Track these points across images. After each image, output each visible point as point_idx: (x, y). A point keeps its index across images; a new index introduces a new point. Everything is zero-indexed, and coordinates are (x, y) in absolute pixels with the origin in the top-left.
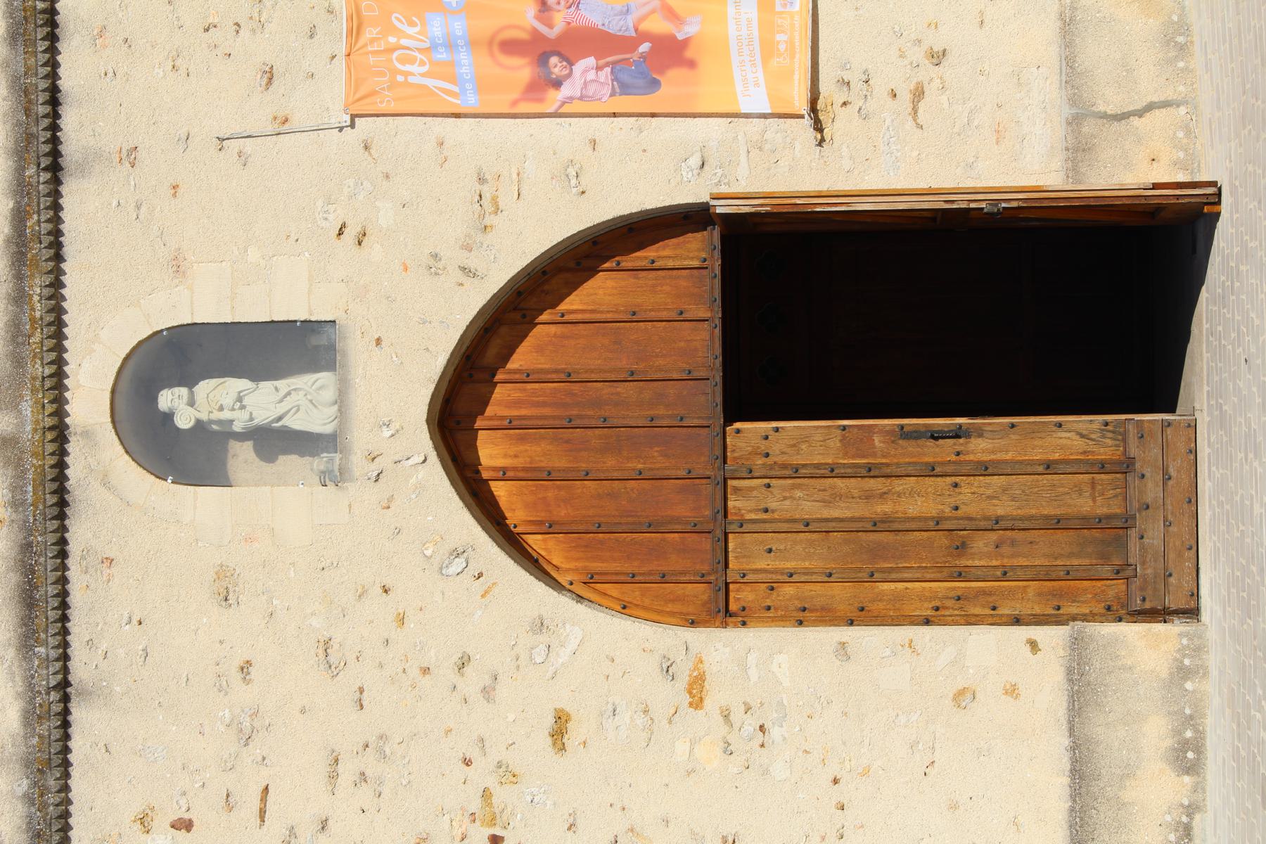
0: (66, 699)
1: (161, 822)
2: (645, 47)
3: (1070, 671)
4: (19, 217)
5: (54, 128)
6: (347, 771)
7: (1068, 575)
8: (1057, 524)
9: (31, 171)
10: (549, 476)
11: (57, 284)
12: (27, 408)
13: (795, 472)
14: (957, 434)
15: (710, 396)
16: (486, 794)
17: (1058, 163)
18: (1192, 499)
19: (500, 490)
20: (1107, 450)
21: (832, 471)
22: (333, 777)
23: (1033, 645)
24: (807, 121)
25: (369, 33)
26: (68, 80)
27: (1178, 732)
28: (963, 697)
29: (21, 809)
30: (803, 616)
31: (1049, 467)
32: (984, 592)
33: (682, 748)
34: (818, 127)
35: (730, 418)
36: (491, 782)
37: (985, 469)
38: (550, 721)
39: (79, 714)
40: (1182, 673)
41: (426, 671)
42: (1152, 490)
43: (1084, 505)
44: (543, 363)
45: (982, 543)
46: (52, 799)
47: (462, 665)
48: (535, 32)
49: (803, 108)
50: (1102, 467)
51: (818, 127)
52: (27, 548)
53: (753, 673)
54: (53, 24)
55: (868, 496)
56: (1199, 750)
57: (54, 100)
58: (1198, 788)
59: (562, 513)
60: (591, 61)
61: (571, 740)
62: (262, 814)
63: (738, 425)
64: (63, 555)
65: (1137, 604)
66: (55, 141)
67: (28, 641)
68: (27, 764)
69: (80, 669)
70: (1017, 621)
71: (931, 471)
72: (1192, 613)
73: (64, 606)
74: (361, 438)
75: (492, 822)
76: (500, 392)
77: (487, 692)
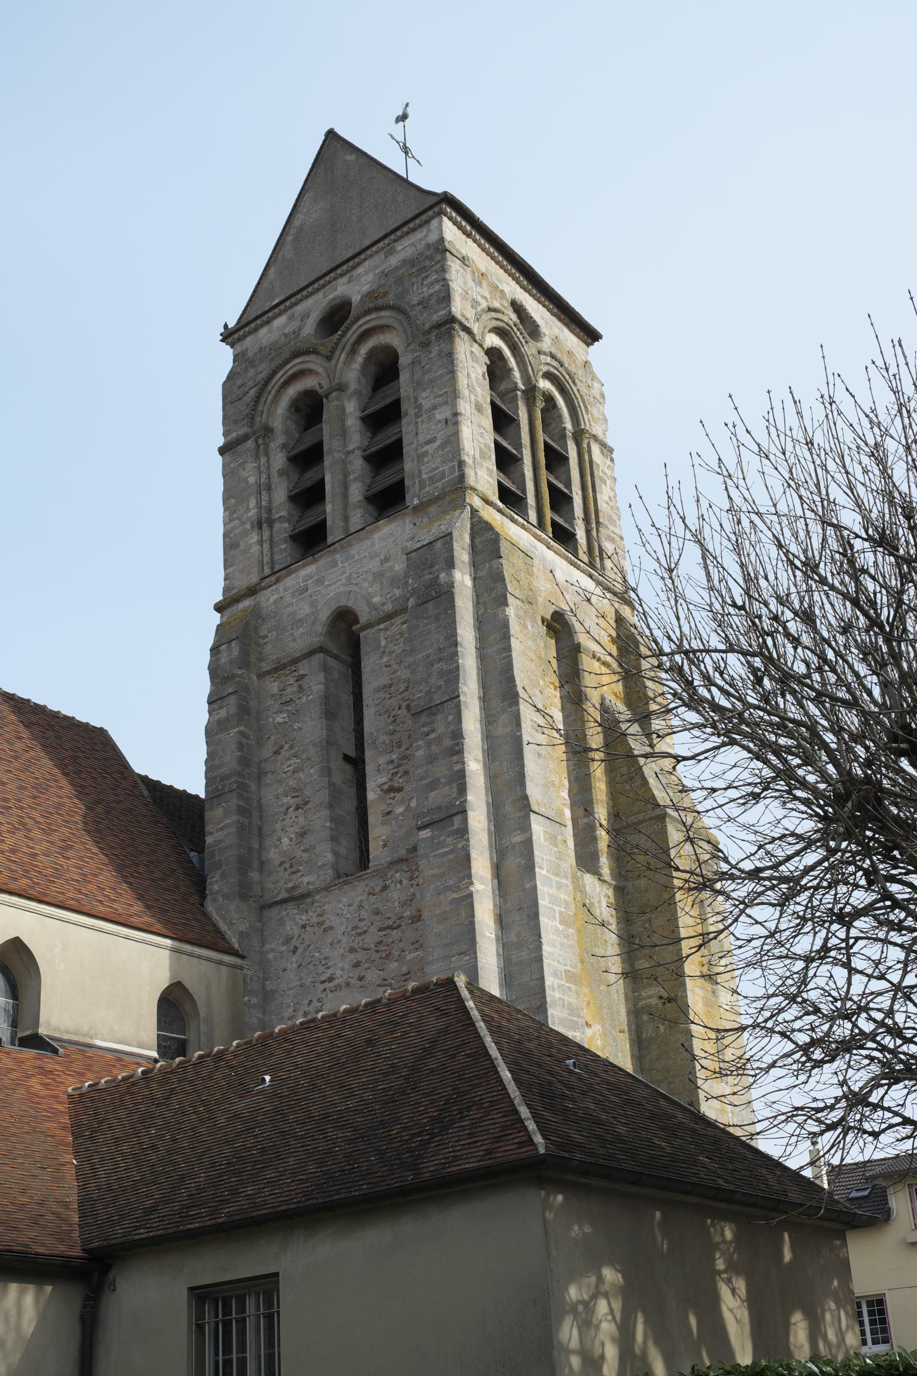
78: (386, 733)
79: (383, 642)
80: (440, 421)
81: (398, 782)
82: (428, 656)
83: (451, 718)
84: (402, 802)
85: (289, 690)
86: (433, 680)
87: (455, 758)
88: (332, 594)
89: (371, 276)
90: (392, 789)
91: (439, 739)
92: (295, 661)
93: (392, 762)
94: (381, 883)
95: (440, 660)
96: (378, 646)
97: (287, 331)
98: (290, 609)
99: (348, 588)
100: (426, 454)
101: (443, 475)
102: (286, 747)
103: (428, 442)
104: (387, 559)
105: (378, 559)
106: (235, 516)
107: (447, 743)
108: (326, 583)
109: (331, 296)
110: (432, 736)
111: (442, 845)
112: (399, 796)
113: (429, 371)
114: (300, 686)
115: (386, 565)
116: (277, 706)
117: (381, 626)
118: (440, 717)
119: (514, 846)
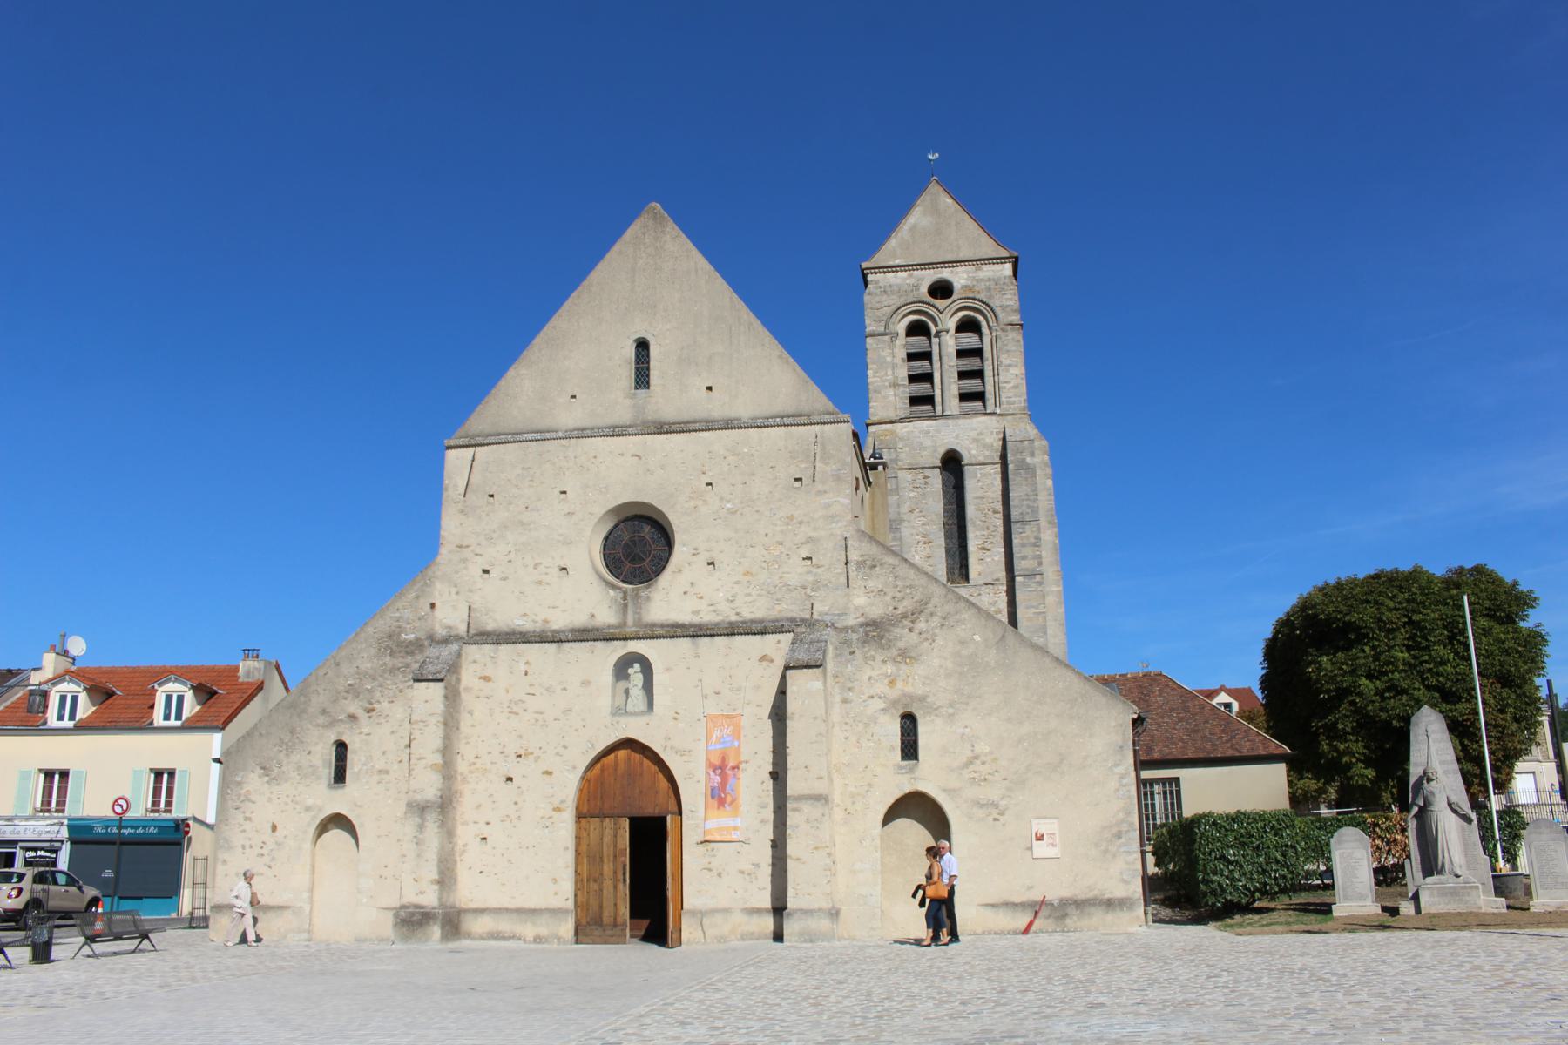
0: (558, 642)
1: (526, 667)
2: (723, 795)
3: (559, 909)
4: (682, 626)
5: (705, 636)
6: (539, 717)
7: (588, 910)
8: (601, 907)
9: (692, 629)
10: (616, 770)
11: (664, 637)
12: (634, 629)
13: (615, 836)
14: (625, 880)
15: (636, 813)
16: (532, 754)
17: (691, 907)
18: (606, 943)
19: (612, 756)
20: (620, 920)
21: (615, 846)
22: (537, 713)
23: (567, 900)
24: (703, 840)
25: (728, 720)
26: (717, 639)
27: (543, 937)
28: (555, 880)
29: (532, 630)
30: (578, 838)
31: (615, 905)
32: (583, 887)
33: (542, 806)
34: (702, 843)
35: (630, 818)
36: (535, 755)
37: (615, 887)
38: (550, 770)
39: (554, 645)
40: (559, 939)
41: (563, 737)
42: (609, 932)
43: (606, 914)
44: (645, 768)
45: (596, 886)
46: (533, 638)
47: (565, 747)
48: (727, 766)
49: (707, 839)
50: (615, 919)
51: (702, 843)
52: (598, 631)
53: (562, 824)
54: (732, 634)
55: (608, 856)
56: (539, 943)
57: (711, 635)
58: (530, 942)
59: (606, 773)
60: (720, 781)
61: (545, 776)
62: (529, 694)
63: (628, 821)
64: (594, 640)
65: (579, 928)
66: (701, 636)
67: (573, 630)
68: (543, 631)
69: (567, 646)
70: (576, 895)
71: (615, 872)
72: (577, 942)
73: (581, 641)
74: (623, 720)
75: (525, 755)
76: (637, 756)
77: (557, 754)
78: (981, 521)
79: (979, 475)
80: (1012, 374)
81: (986, 545)
82: (1021, 496)
83: (1034, 529)
84: (990, 556)
85: (918, 481)
86: (1024, 508)
87: (1037, 548)
88: (946, 441)
89: (965, 276)
90: (984, 549)
91: (1027, 537)
92: (924, 468)
93: (984, 535)
94: (978, 592)
95: (1027, 500)
96: (976, 476)
97: (907, 282)
98: (918, 440)
99: (958, 441)
100: (1005, 388)
101: (1014, 403)
102: (917, 510)
103: (1006, 382)
104: (981, 434)
105: (976, 432)
106: (878, 375)
107: (1032, 540)
108: (942, 433)
109: (940, 276)
110: (1023, 535)
111: (1029, 586)
112: (988, 553)
113: (1006, 345)
114: (926, 483)
115: (981, 437)
116: (911, 488)
117: (978, 467)
118: (1027, 527)
119: (1053, 591)
